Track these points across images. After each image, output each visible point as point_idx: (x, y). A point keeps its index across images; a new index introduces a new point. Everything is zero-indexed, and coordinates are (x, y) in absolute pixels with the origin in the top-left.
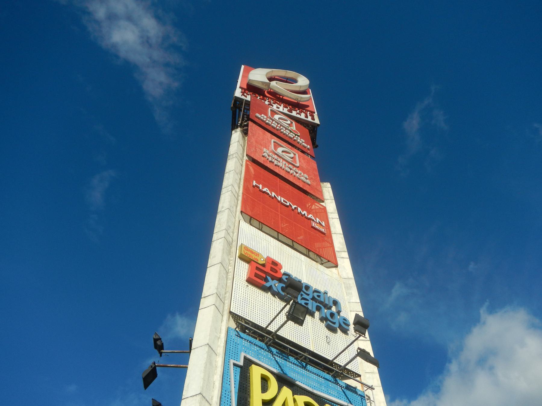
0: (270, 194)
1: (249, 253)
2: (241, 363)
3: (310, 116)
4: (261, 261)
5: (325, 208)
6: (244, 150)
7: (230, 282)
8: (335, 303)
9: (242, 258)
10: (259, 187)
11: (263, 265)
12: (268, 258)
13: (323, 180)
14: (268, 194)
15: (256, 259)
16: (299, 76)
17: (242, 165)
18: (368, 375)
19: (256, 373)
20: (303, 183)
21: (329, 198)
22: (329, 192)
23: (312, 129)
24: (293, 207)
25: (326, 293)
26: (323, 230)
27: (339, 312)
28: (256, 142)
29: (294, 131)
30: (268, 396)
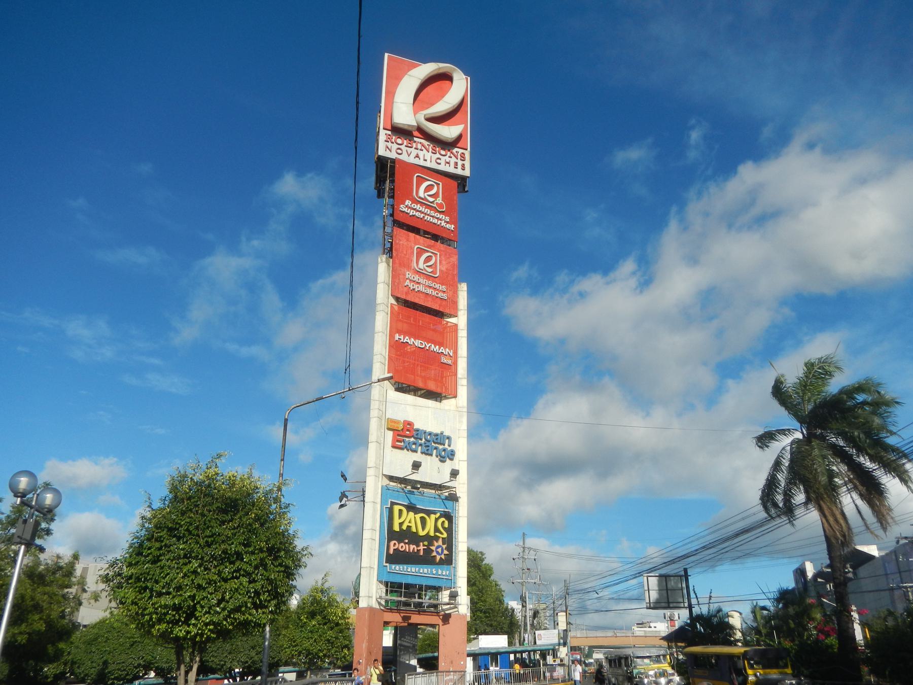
0: (410, 343)
1: (393, 424)
2: (389, 506)
3: (461, 160)
4: (401, 427)
5: (456, 325)
6: (389, 286)
7: (382, 451)
8: (449, 438)
9: (389, 429)
10: (401, 339)
11: (402, 429)
12: (405, 421)
13: (461, 281)
14: (408, 343)
15: (397, 427)
16: (455, 70)
17: (387, 314)
18: (461, 485)
19: (396, 508)
20: (439, 302)
21: (463, 309)
22: (464, 299)
23: (461, 181)
24: (428, 346)
25: (442, 433)
26: (449, 362)
27: (449, 446)
28: (400, 264)
29: (440, 205)
30: (401, 521)
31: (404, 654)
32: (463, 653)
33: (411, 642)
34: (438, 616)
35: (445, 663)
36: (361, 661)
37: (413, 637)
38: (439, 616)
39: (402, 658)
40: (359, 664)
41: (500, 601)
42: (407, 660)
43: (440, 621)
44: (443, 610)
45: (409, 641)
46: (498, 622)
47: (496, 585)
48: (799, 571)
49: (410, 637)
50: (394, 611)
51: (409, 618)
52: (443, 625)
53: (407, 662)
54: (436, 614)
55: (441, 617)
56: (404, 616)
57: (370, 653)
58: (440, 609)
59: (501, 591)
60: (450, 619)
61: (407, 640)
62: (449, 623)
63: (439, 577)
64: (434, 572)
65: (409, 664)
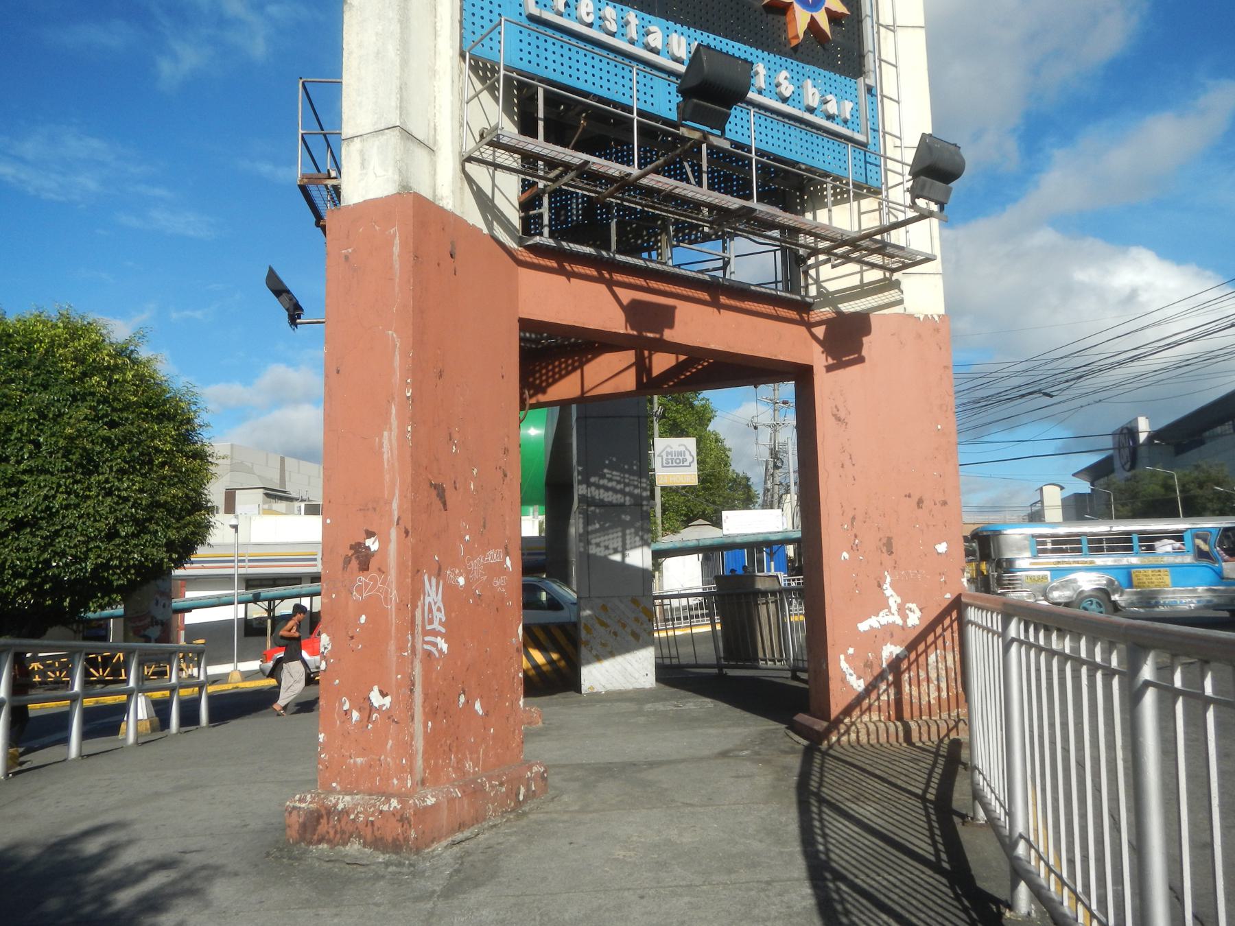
31: (603, 530)
32: (945, 503)
33: (627, 489)
34: (802, 322)
35: (853, 549)
36: (373, 544)
37: (631, 472)
38: (809, 326)
39: (598, 545)
40: (364, 567)
41: (726, 465)
42: (616, 551)
43: (818, 349)
44: (827, 298)
45: (619, 487)
46: (725, 498)
47: (717, 440)
48: (1125, 431)
49: (622, 471)
50: (579, 269)
51: (666, 317)
52: (829, 369)
53: (617, 557)
54: (793, 315)
55: (820, 331)
56: (635, 304)
57: (440, 492)
58: (813, 291)
59: (724, 450)
60: (865, 340)
61: (610, 485)
62: (861, 360)
63: (808, 116)
64: (787, 89)
65: (623, 566)
